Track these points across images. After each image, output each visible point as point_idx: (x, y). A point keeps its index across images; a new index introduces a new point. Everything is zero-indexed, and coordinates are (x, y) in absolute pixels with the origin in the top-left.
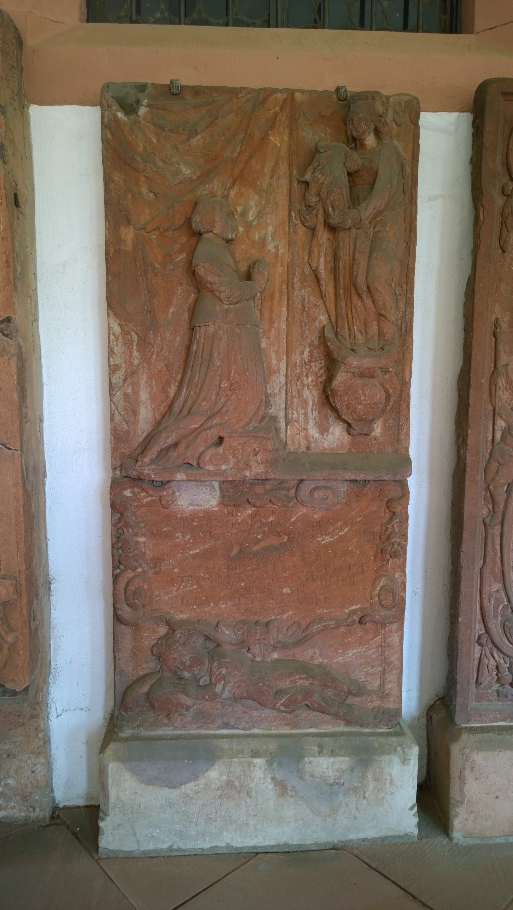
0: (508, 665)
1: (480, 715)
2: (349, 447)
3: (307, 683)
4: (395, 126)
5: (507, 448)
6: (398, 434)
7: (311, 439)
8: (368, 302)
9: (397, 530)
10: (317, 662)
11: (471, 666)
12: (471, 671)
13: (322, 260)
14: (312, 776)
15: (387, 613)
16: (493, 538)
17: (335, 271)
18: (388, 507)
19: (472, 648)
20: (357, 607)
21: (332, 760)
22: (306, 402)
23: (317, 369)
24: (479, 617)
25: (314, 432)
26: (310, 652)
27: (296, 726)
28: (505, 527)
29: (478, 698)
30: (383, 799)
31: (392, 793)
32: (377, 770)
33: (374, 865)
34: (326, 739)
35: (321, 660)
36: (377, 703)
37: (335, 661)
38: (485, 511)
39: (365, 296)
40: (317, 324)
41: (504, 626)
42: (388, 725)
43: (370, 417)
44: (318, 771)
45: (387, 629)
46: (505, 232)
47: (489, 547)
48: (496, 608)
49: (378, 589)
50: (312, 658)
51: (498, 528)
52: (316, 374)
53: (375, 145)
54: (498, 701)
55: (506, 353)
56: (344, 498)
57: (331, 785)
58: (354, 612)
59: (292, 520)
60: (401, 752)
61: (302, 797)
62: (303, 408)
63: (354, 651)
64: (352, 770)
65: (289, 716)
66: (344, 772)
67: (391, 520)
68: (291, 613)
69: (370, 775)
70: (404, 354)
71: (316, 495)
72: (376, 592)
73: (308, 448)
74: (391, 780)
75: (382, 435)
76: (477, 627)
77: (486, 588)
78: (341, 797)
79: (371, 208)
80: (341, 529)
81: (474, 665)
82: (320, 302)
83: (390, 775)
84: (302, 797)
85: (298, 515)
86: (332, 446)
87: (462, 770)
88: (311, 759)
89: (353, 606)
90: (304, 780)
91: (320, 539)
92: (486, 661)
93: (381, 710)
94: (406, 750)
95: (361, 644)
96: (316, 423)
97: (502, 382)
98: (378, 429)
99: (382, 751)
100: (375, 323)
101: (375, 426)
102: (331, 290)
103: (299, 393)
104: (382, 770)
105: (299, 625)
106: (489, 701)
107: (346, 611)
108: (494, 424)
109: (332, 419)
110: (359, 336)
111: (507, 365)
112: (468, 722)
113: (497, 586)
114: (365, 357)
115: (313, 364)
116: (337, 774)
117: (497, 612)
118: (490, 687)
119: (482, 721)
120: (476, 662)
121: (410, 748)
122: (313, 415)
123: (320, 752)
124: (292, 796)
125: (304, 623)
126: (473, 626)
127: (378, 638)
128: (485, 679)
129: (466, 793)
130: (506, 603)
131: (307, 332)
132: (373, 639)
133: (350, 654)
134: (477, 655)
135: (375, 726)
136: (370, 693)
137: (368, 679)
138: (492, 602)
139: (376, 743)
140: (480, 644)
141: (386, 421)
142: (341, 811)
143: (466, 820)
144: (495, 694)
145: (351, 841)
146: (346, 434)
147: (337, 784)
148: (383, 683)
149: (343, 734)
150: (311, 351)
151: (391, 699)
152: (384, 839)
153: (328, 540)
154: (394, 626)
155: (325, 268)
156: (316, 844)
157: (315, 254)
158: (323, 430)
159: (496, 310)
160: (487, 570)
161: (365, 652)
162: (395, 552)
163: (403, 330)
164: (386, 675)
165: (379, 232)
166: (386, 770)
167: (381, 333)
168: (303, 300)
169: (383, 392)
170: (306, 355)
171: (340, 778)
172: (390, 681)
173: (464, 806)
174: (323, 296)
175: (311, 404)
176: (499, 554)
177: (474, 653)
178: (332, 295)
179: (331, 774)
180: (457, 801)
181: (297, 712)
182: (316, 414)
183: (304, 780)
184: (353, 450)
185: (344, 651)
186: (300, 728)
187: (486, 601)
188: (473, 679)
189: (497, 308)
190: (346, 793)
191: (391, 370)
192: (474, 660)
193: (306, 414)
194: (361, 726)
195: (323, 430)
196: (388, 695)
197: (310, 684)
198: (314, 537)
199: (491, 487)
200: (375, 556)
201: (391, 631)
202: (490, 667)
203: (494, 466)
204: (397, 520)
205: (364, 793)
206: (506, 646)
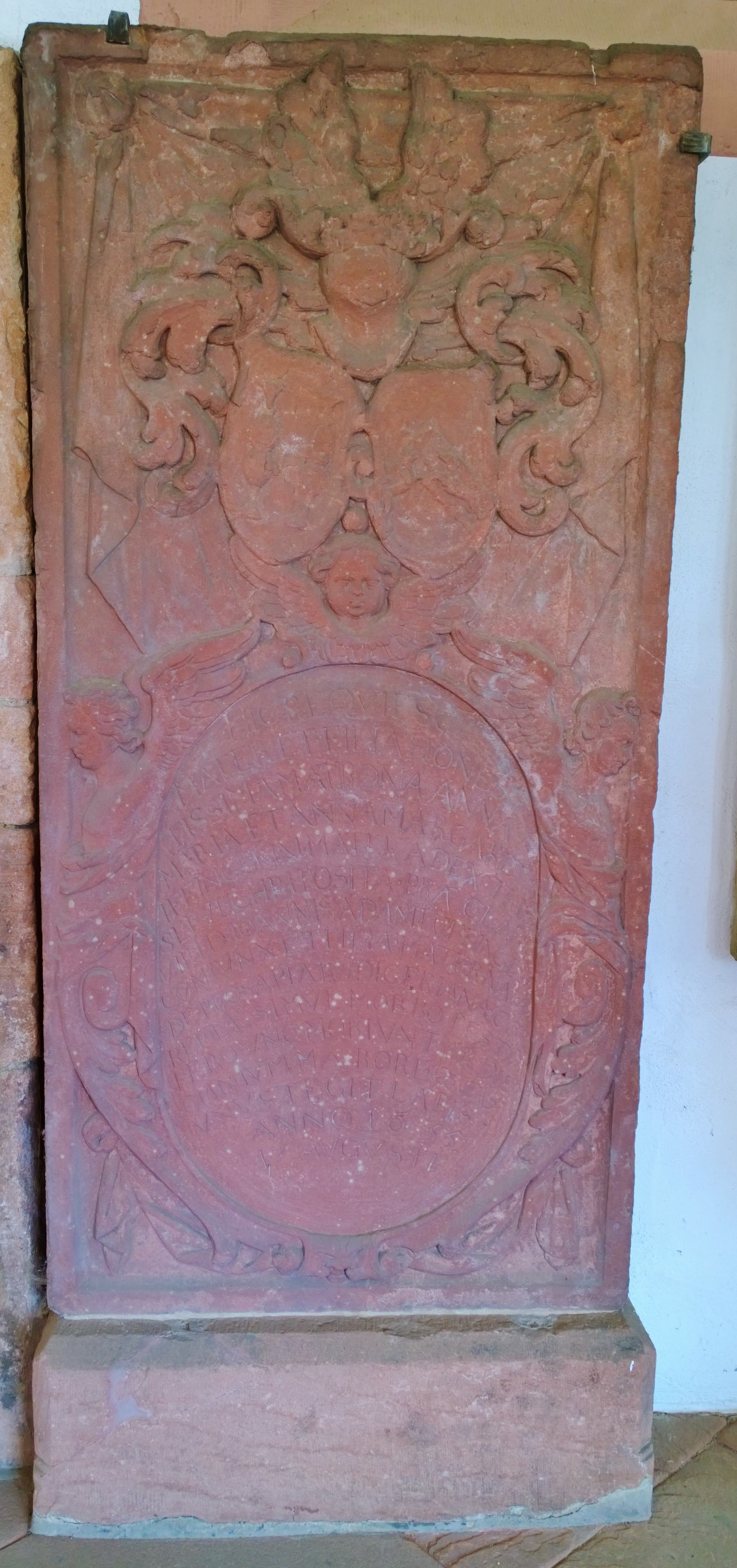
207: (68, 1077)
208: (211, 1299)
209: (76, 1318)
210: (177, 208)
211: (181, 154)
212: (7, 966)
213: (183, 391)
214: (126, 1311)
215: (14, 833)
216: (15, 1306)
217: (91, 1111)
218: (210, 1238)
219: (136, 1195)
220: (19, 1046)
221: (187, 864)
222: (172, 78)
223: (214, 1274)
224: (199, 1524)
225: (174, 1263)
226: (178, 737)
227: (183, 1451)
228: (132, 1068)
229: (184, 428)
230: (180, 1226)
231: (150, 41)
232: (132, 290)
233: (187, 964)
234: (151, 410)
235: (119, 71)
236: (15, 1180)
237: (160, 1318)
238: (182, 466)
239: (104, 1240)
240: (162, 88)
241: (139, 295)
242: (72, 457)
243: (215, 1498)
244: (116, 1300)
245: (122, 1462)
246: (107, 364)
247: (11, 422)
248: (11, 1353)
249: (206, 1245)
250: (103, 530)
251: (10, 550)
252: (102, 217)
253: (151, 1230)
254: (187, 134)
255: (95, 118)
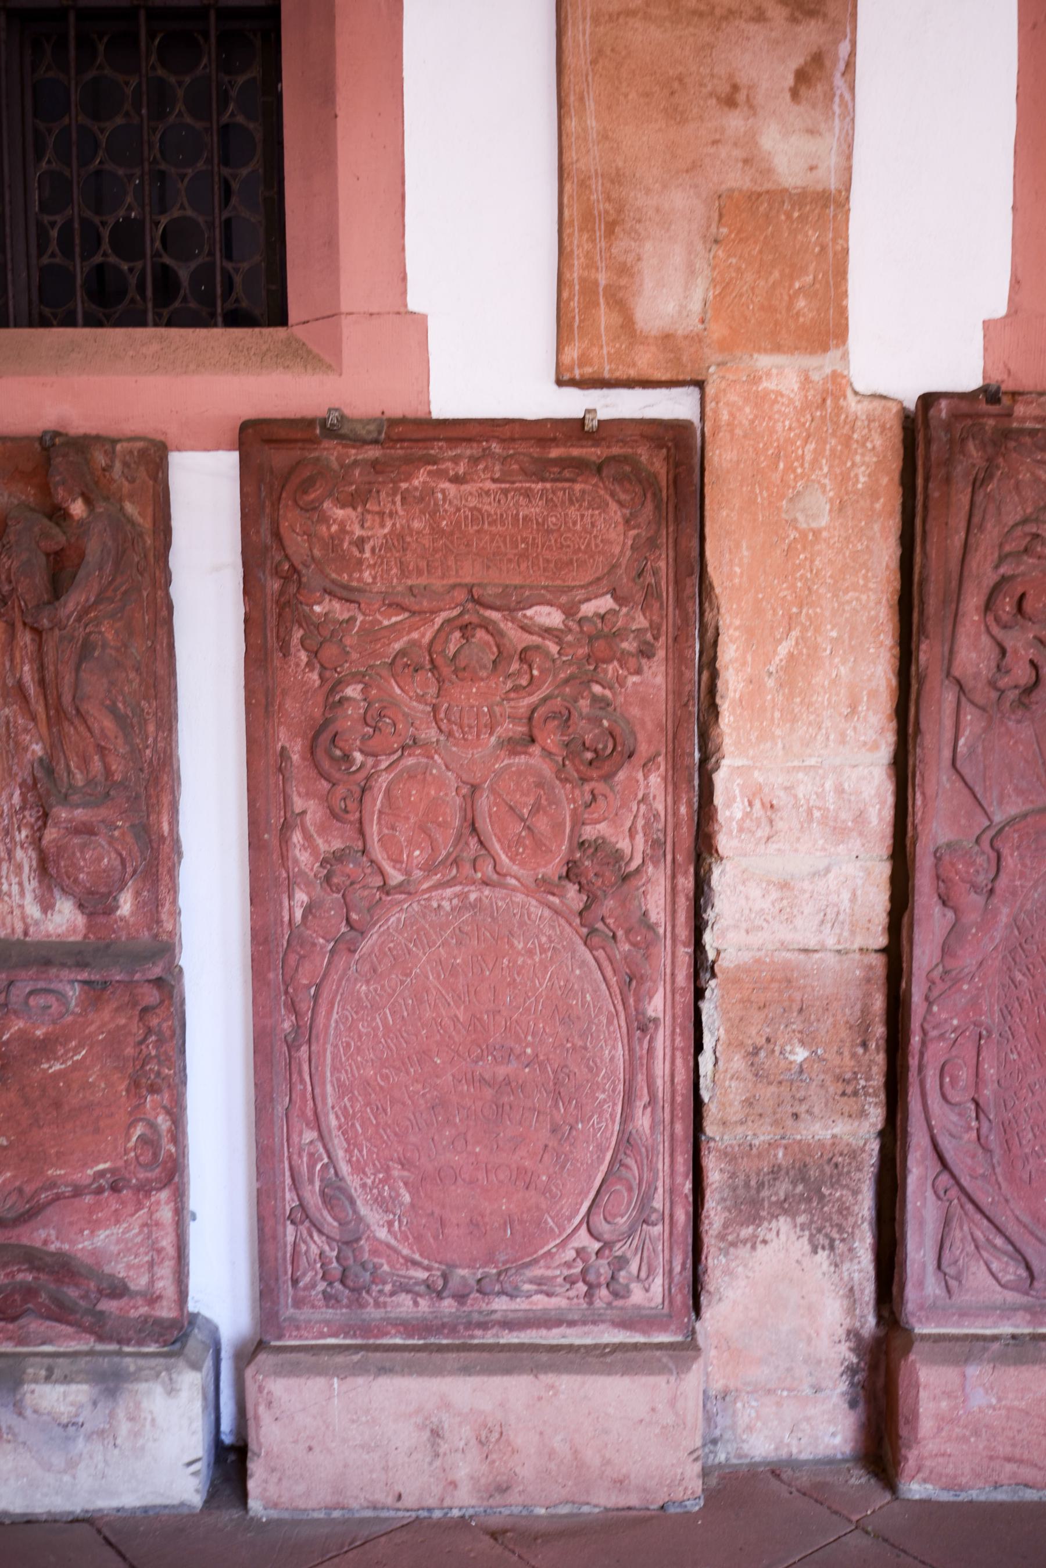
0: (335, 1253)
1: (298, 1328)
2: (84, 932)
3: (30, 1278)
4: (126, 484)
5: (309, 932)
6: (158, 912)
7: (29, 920)
8: (82, 729)
9: (153, 1053)
10: (52, 1248)
11: (280, 1255)
12: (280, 1261)
13: (26, 668)
14: (35, 1411)
15: (149, 1175)
16: (300, 1065)
17: (42, 683)
18: (141, 1019)
19: (280, 1229)
20: (107, 1165)
21: (60, 1389)
22: (19, 867)
23: (33, 820)
24: (288, 1181)
25: (33, 911)
26: (43, 1234)
27: (21, 1342)
28: (313, 1048)
29: (298, 1303)
30: (143, 1448)
31: (155, 1440)
32: (131, 1404)
33: (113, 1540)
34: (61, 1360)
35: (58, 1244)
36: (144, 1310)
37: (80, 1246)
38: (286, 1025)
39: (76, 721)
40: (29, 756)
41: (323, 1194)
42: (157, 1342)
43: (103, 890)
44: (45, 1405)
45: (153, 1199)
46: (282, 630)
47: (295, 1077)
48: (311, 1167)
49: (134, 1139)
50: (45, 1242)
51: (304, 1048)
52: (32, 827)
53: (85, 515)
54: (327, 1307)
55: (299, 794)
56: (77, 1005)
57: (66, 1426)
58: (101, 1174)
59: (5, 1038)
60: (167, 1379)
61: (24, 1443)
62: (16, 875)
63: (108, 1232)
64: (95, 1404)
65: (11, 1326)
66: (82, 1406)
67: (145, 1039)
68: (8, 1174)
69: (121, 1414)
70: (157, 796)
71: (32, 1002)
72: (131, 1144)
73: (26, 933)
74: (153, 1420)
75: (132, 914)
76: (288, 1196)
77: (295, 1138)
78: (80, 1443)
79: (71, 605)
80: (76, 1050)
81: (285, 1253)
82: (31, 725)
83: (151, 1412)
84: (24, 1443)
85: (12, 1030)
86: (59, 931)
87: (256, 1405)
88: (33, 1386)
89: (98, 1163)
90: (24, 1418)
91: (45, 1066)
92: (304, 1248)
93: (151, 1321)
94: (174, 1376)
95: (117, 1222)
96: (36, 897)
97: (297, 837)
98: (126, 905)
99: (135, 1377)
100: (96, 758)
101: (122, 901)
102: (40, 709)
103: (9, 854)
104: (138, 1405)
105: (20, 1191)
106: (313, 1306)
107: (90, 1172)
108: (290, 898)
109: (57, 893)
110: (79, 776)
111: (304, 812)
112: (280, 1337)
113: (310, 1135)
114: (77, 806)
115: (27, 813)
116: (73, 1409)
117: (313, 1174)
118: (313, 1285)
119: (301, 1337)
120: (289, 1249)
121: (179, 1373)
122: (31, 885)
123: (48, 1379)
124: (9, 1441)
125: (28, 1189)
126: (279, 1194)
127: (141, 1213)
128: (304, 1274)
129: (262, 1440)
130: (326, 1160)
131: (15, 768)
132: (132, 1215)
133: (102, 1237)
134: (290, 1239)
135: (140, 1343)
136: (133, 1295)
137: (131, 1273)
138: (305, 1159)
139: (130, 1364)
140: (293, 1222)
141: (137, 894)
142: (82, 1465)
143: (266, 1481)
144: (320, 1296)
145: (100, 1510)
146: (78, 912)
147: (74, 1424)
148: (152, 1282)
149: (91, 1353)
150: (23, 795)
151: (165, 1303)
152: (145, 1509)
153: (58, 1067)
154: (164, 1195)
155: (33, 679)
156: (49, 1513)
157: (18, 660)
158: (47, 907)
159: (281, 736)
160: (295, 1114)
161: (123, 1233)
162: (152, 1085)
163: (155, 763)
164: (155, 1268)
165: (90, 633)
166: (145, 1404)
167: (108, 772)
168: (8, 723)
169: (113, 855)
170: (16, 799)
171: (77, 1415)
172: (162, 1278)
173: (261, 1460)
174: (34, 718)
175: (26, 869)
176: (309, 1088)
177: (285, 1235)
178: (44, 717)
179: (64, 1410)
180: (254, 1454)
181: (22, 1321)
182: (35, 883)
183: (24, 1418)
184: (91, 936)
185: (92, 1232)
186: (27, 1344)
187: (295, 1157)
188: (286, 1273)
189: (283, 735)
190: (89, 1438)
191: (120, 823)
192: (285, 1246)
193: (20, 884)
194: (120, 1342)
195: (47, 907)
196: (160, 1297)
197: (35, 1278)
198: (37, 1062)
199: (291, 990)
200: (128, 1091)
201: (158, 1202)
202: (313, 1257)
203: (293, 959)
204: (153, 1038)
205: (115, 1438)
206: (329, 1224)
207: (925, 1142)
208: (1028, 1317)
209: (926, 1331)
210: (1029, 510)
211: (1033, 474)
212: (867, 1057)
213: (1031, 636)
214: (963, 1326)
215: (874, 956)
216: (862, 1327)
217: (939, 1167)
218: (1028, 1268)
219: (972, 1234)
220: (873, 1120)
221: (1019, 977)
222: (1028, 425)
223: (1030, 1299)
224: (1029, 1491)
225: (998, 1288)
226: (1018, 883)
227: (1019, 1431)
228: (974, 1134)
229: (1032, 662)
230: (1005, 1259)
231: (1014, 401)
232: (997, 567)
233: (1019, 1054)
234: (1009, 650)
235: (991, 422)
236: (866, 1226)
237: (988, 1332)
238: (1029, 690)
239: (947, 1270)
240: (1021, 431)
241: (1002, 570)
242: (947, 682)
243: (1040, 1469)
244: (955, 1318)
245: (972, 1440)
246: (976, 618)
247: (888, 655)
248: (858, 1363)
249: (1024, 1274)
250: (967, 733)
251: (883, 747)
252: (976, 520)
253: (982, 1263)
254: (1038, 462)
255: (974, 453)
